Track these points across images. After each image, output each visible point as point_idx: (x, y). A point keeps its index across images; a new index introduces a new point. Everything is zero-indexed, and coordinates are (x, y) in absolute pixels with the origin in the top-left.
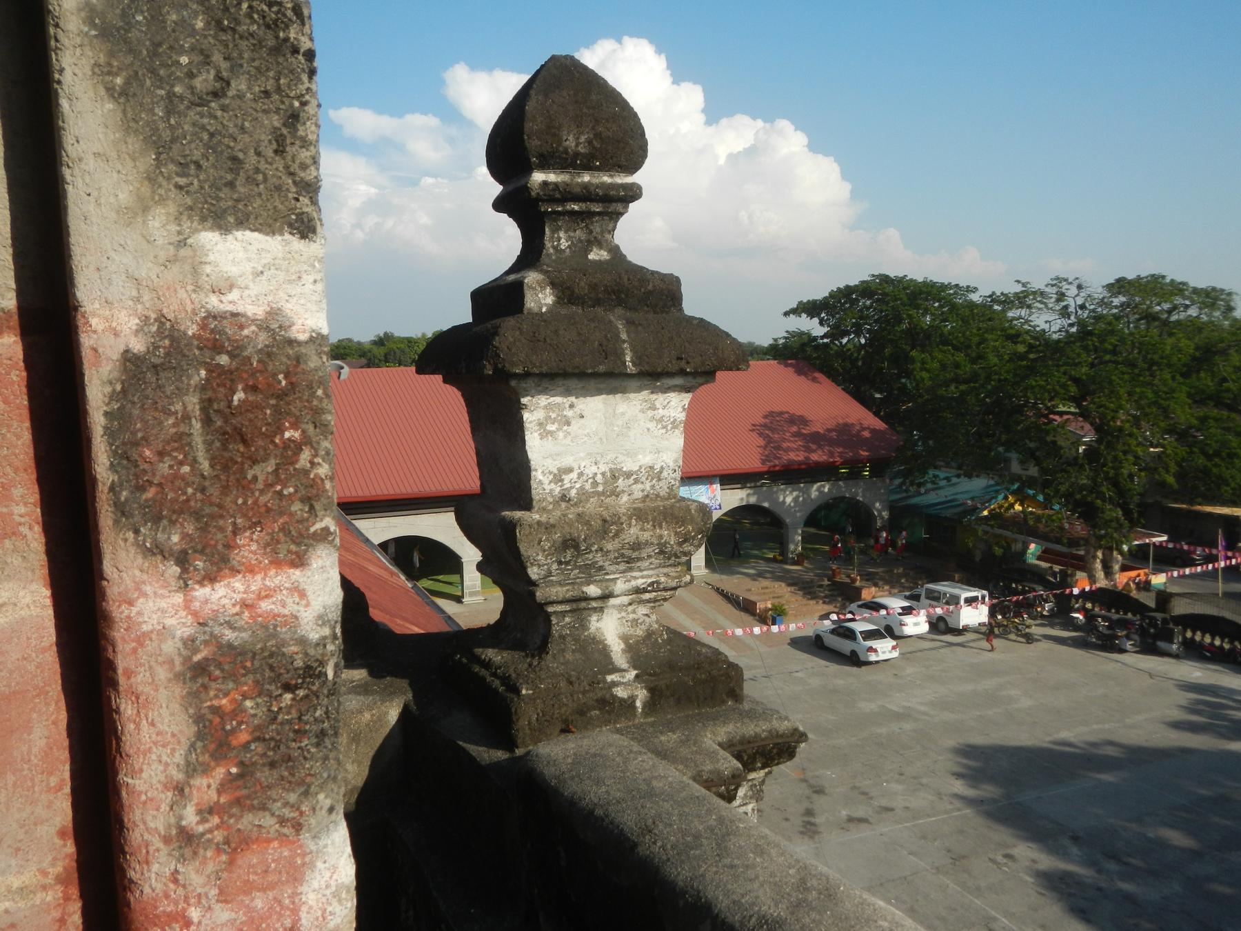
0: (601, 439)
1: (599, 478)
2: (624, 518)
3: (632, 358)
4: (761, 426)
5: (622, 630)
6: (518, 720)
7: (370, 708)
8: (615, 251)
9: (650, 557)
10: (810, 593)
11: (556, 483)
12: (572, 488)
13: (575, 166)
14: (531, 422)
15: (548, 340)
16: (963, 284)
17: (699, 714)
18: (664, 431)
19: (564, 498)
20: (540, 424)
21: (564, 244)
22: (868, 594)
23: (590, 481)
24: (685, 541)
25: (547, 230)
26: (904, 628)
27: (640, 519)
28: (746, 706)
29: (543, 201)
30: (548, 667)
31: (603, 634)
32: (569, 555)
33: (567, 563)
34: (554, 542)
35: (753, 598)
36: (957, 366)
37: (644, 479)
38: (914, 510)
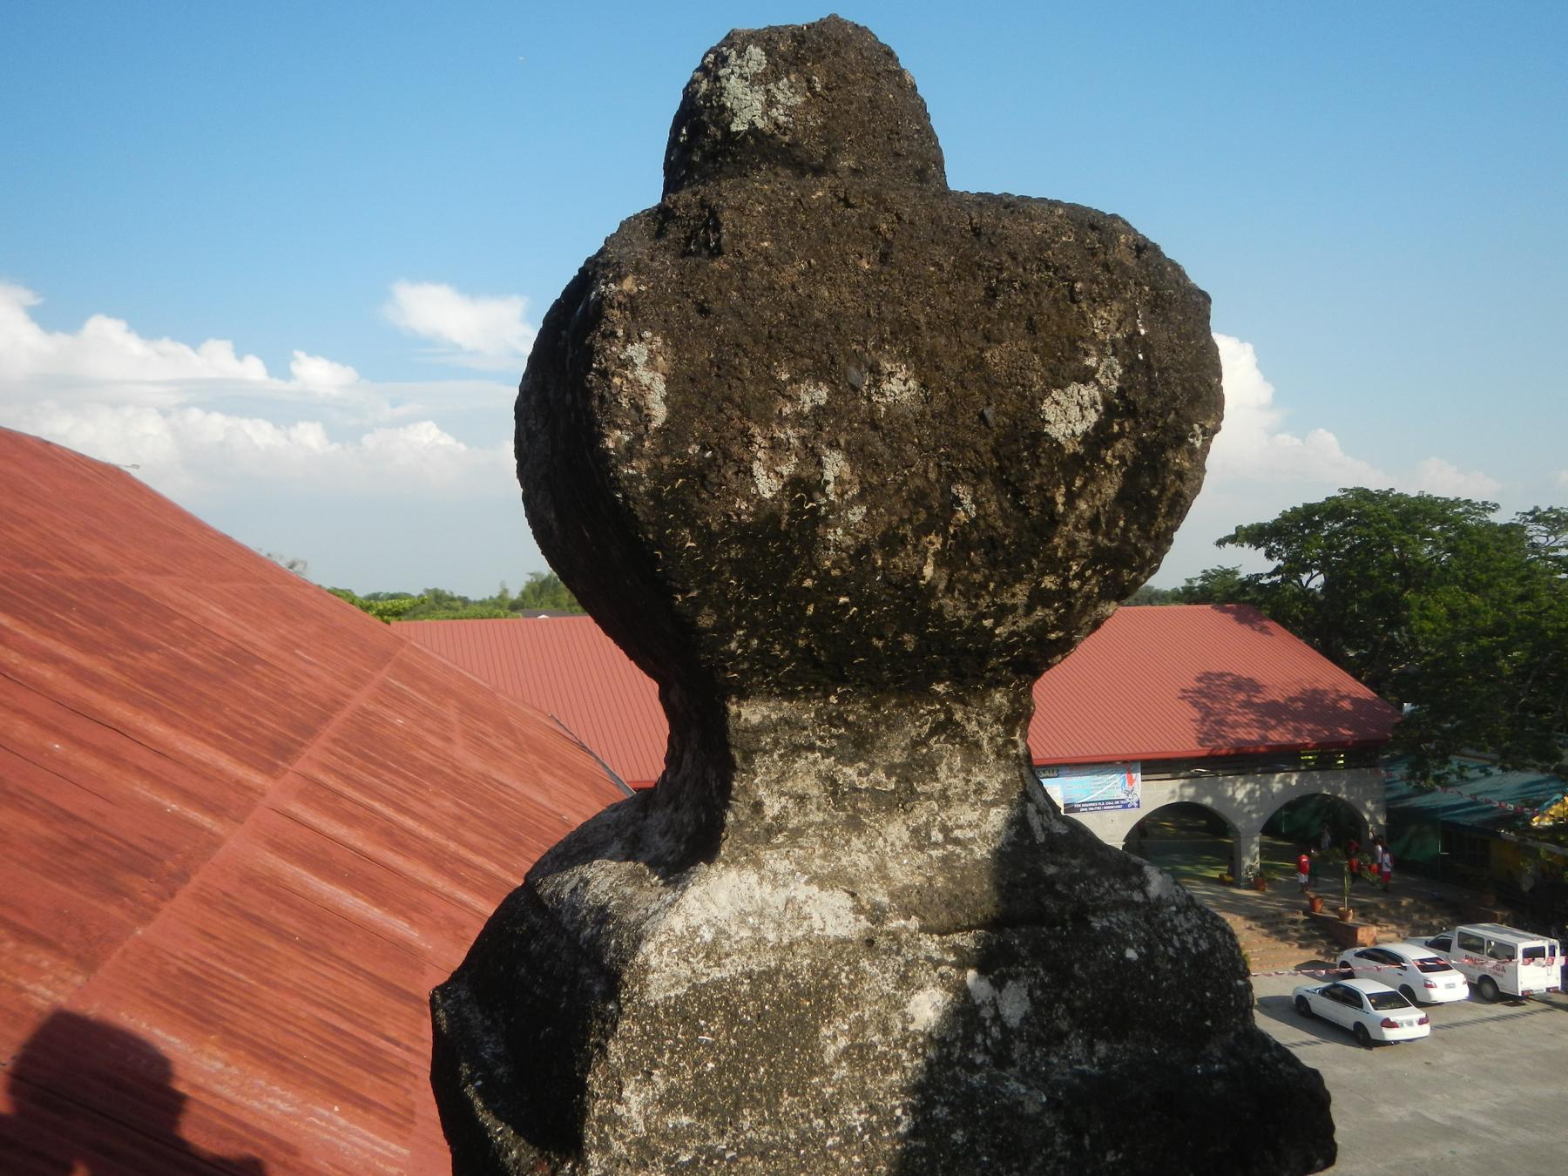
4: (1194, 691)
10: (1278, 932)
16: (1477, 499)
22: (1367, 935)
26: (1432, 991)
36: (1475, 611)
38: (1425, 816)
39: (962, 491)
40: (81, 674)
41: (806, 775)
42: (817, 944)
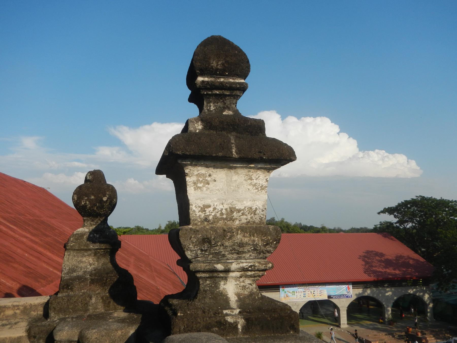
0: (225, 192)
1: (224, 211)
2: (235, 230)
3: (236, 151)
5: (237, 291)
6: (173, 328)
7: (121, 329)
8: (237, 112)
9: (249, 251)
11: (202, 212)
12: (210, 215)
13: (217, 75)
14: (190, 182)
15: (195, 141)
17: (273, 336)
18: (257, 190)
19: (206, 219)
20: (195, 183)
21: (212, 108)
23: (219, 212)
24: (267, 244)
25: (205, 102)
27: (243, 231)
28: (301, 335)
29: (202, 89)
30: (195, 305)
31: (226, 291)
32: (206, 246)
33: (206, 251)
34: (198, 239)
35: (370, 340)
37: (247, 213)
39: (97, 204)
40: (32, 241)
41: (89, 223)
42: (85, 232)
